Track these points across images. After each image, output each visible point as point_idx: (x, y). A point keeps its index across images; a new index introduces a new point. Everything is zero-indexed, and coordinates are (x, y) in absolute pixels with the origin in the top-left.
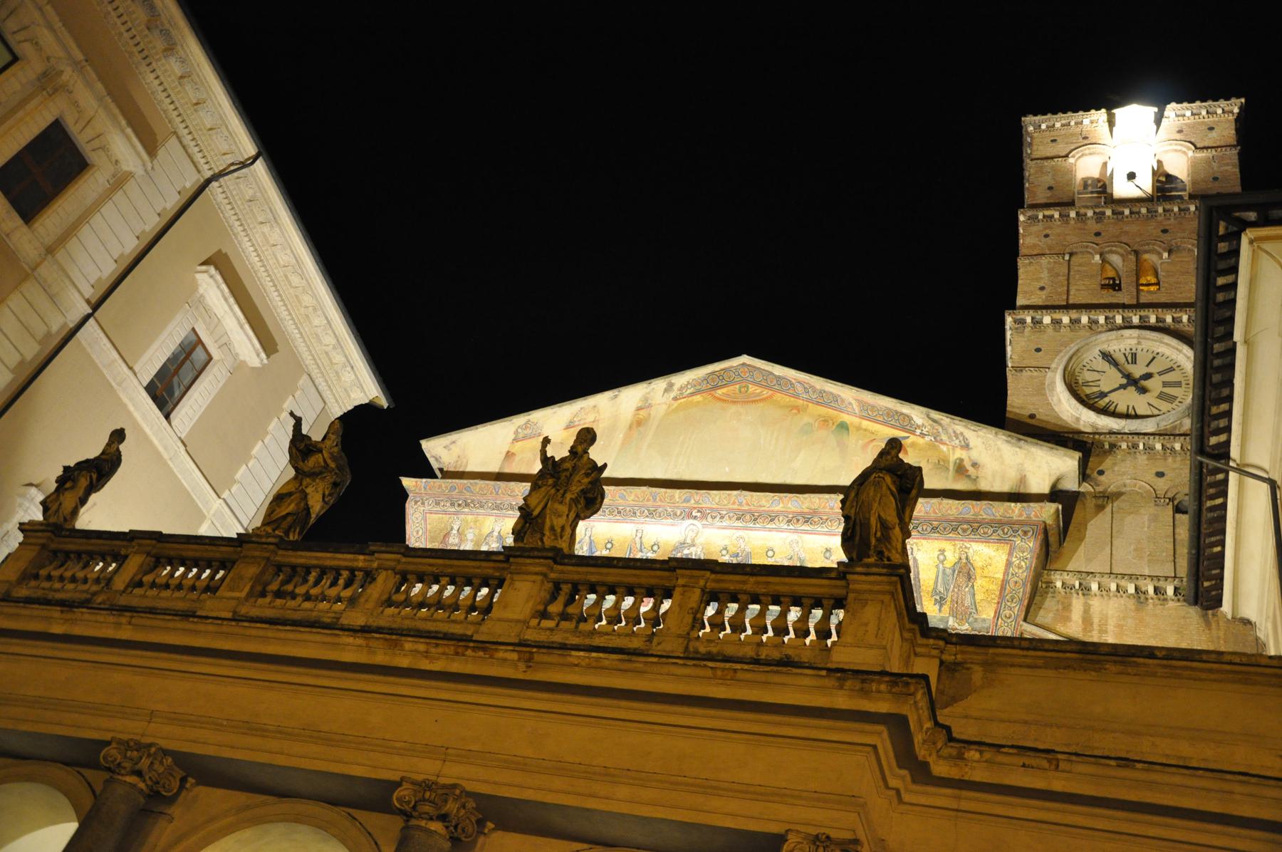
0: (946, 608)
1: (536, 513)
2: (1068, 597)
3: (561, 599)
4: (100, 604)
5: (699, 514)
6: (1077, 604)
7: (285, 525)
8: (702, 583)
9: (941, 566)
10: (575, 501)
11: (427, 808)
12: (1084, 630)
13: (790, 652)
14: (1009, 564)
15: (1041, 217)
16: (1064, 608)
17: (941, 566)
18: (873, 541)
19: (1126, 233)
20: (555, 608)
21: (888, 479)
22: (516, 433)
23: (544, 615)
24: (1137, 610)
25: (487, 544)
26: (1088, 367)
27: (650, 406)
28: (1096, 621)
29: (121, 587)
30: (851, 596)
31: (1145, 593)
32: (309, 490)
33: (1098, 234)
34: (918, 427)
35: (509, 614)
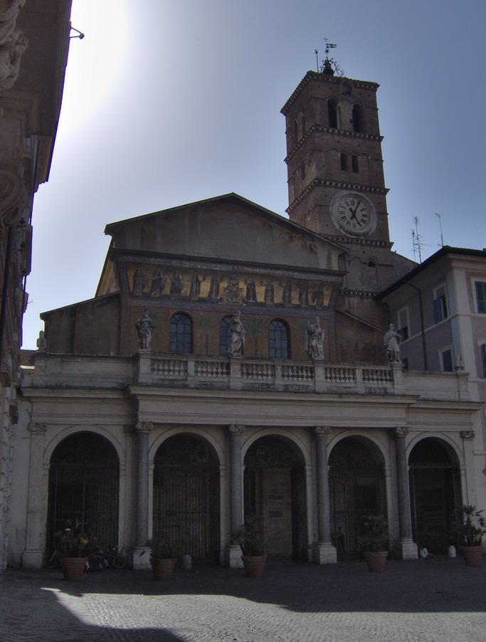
0: (315, 304)
2: (344, 296)
6: (346, 299)
11: (323, 432)
14: (333, 290)
15: (320, 129)
33: (339, 142)
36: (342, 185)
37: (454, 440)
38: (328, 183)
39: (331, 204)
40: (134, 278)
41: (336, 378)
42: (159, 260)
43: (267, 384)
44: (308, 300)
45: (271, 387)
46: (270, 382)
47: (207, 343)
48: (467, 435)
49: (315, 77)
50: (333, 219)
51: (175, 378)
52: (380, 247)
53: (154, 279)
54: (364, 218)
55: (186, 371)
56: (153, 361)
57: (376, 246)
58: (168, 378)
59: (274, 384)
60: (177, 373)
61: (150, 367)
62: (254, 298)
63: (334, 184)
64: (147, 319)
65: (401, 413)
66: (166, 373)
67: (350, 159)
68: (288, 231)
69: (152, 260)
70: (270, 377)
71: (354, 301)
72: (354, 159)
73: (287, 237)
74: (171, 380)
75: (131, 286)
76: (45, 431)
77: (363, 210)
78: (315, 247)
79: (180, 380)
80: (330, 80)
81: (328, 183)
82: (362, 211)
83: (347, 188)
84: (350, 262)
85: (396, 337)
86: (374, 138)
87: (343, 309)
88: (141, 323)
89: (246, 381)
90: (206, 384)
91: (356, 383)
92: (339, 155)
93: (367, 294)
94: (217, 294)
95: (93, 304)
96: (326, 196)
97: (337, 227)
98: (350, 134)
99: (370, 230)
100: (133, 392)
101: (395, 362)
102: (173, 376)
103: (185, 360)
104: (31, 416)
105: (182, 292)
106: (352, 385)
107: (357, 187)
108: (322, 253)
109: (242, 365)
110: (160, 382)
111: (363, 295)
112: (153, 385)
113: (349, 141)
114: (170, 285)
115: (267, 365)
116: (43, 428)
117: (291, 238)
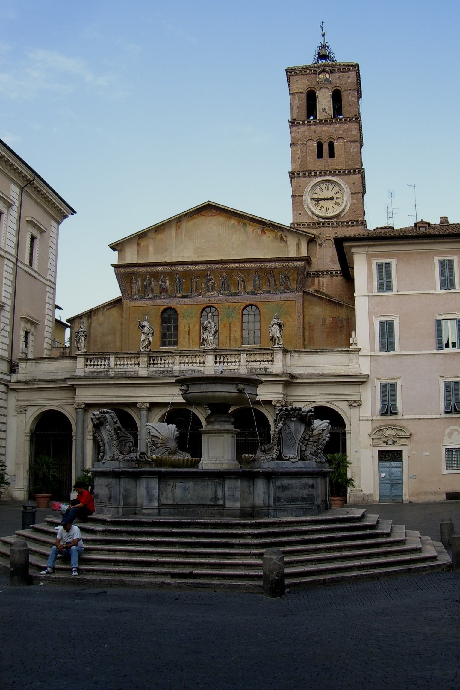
0: (283, 287)
1: (206, 339)
2: (313, 277)
3: (218, 358)
4: (111, 372)
5: (210, 267)
6: (316, 279)
7: (146, 347)
8: (246, 353)
9: (281, 275)
10: (213, 335)
12: (318, 287)
13: (266, 366)
15: (296, 123)
16: (313, 281)
17: (281, 275)
18: (276, 341)
19: (323, 131)
20: (218, 360)
21: (277, 326)
22: (139, 236)
23: (216, 363)
24: (331, 279)
25: (146, 282)
26: (315, 193)
27: (181, 221)
28: (321, 284)
29: (114, 367)
30: (274, 353)
31: (333, 274)
32: (149, 338)
33: (315, 132)
34: (267, 225)
35: (209, 364)
36: (315, 173)
37: (342, 408)
38: (301, 174)
39: (305, 193)
40: (131, 285)
41: (224, 362)
42: (145, 268)
43: (168, 371)
44: (276, 285)
45: (170, 373)
46: (170, 369)
47: (189, 331)
48: (356, 404)
49: (293, 73)
50: (306, 207)
51: (100, 370)
52: (352, 226)
53: (145, 283)
54: (338, 201)
55: (108, 365)
56: (87, 360)
57: (348, 226)
58: (96, 370)
59: (172, 371)
60: (103, 367)
61: (84, 364)
62: (229, 289)
63: (307, 173)
64: (82, 329)
65: (280, 389)
66: (95, 367)
67: (326, 147)
68: (261, 226)
69: (142, 269)
70: (170, 365)
71: (324, 280)
72: (331, 145)
73: (260, 232)
74: (98, 372)
75: (130, 291)
76: (26, 410)
77: (338, 192)
78: (285, 236)
79: (104, 372)
80: (308, 72)
81: (301, 174)
82: (335, 194)
83: (320, 175)
84: (321, 245)
85: (277, 324)
86: (351, 119)
87: (311, 290)
88: (78, 332)
89: (151, 370)
90: (122, 373)
91: (239, 366)
92: (315, 144)
93: (336, 273)
94: (197, 290)
95: (103, 309)
96: (300, 186)
97: (310, 213)
98: (326, 121)
99: (343, 211)
100: (68, 383)
101: (276, 346)
102: (99, 369)
103: (109, 356)
104: (17, 401)
105: (169, 291)
106: (236, 367)
107: (330, 172)
108: (292, 241)
109: (150, 358)
110: (90, 375)
111: (332, 273)
112: (85, 378)
113: (325, 128)
114: (159, 286)
115: (169, 356)
116: (22, 410)
117: (263, 232)
